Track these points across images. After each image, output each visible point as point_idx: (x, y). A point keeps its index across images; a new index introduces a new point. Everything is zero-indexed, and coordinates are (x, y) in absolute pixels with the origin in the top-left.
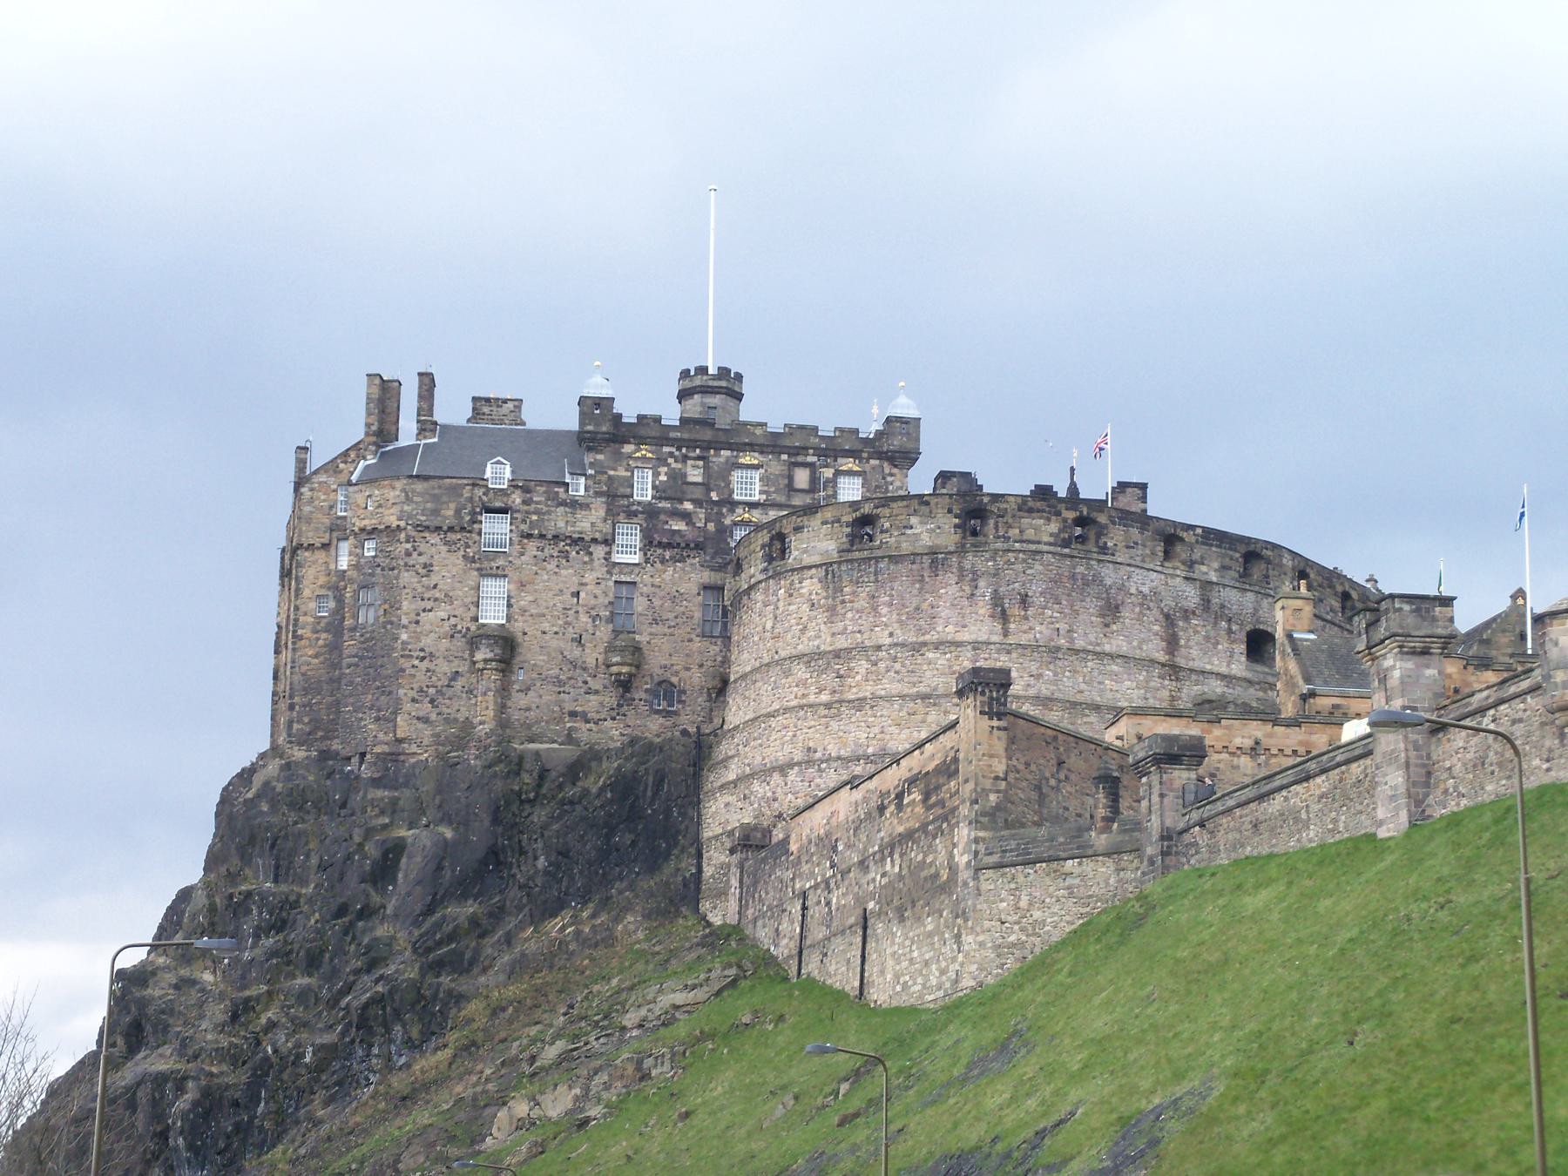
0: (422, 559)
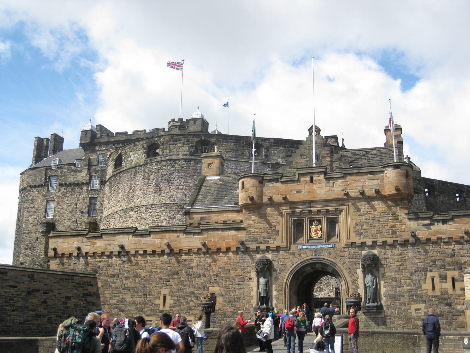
0: (31, 198)
